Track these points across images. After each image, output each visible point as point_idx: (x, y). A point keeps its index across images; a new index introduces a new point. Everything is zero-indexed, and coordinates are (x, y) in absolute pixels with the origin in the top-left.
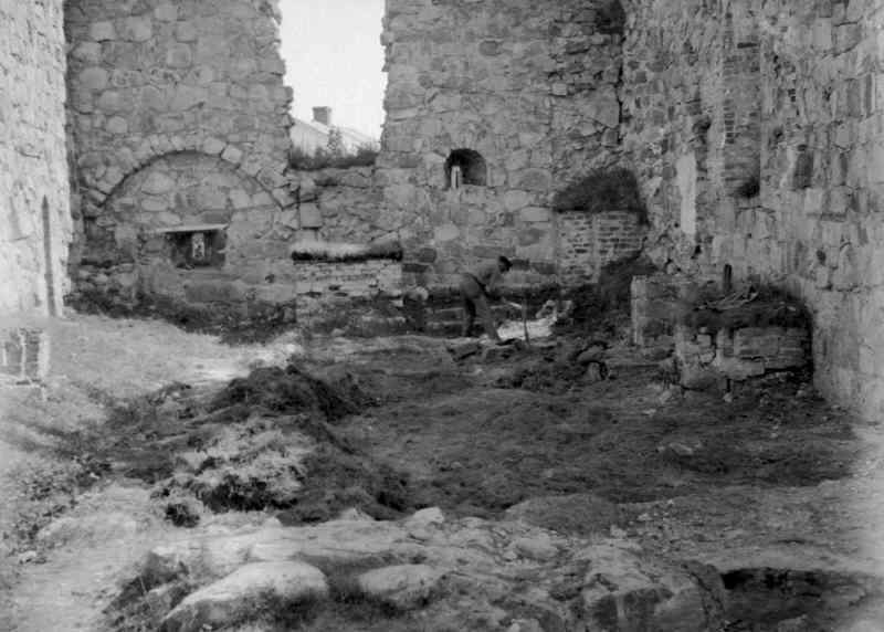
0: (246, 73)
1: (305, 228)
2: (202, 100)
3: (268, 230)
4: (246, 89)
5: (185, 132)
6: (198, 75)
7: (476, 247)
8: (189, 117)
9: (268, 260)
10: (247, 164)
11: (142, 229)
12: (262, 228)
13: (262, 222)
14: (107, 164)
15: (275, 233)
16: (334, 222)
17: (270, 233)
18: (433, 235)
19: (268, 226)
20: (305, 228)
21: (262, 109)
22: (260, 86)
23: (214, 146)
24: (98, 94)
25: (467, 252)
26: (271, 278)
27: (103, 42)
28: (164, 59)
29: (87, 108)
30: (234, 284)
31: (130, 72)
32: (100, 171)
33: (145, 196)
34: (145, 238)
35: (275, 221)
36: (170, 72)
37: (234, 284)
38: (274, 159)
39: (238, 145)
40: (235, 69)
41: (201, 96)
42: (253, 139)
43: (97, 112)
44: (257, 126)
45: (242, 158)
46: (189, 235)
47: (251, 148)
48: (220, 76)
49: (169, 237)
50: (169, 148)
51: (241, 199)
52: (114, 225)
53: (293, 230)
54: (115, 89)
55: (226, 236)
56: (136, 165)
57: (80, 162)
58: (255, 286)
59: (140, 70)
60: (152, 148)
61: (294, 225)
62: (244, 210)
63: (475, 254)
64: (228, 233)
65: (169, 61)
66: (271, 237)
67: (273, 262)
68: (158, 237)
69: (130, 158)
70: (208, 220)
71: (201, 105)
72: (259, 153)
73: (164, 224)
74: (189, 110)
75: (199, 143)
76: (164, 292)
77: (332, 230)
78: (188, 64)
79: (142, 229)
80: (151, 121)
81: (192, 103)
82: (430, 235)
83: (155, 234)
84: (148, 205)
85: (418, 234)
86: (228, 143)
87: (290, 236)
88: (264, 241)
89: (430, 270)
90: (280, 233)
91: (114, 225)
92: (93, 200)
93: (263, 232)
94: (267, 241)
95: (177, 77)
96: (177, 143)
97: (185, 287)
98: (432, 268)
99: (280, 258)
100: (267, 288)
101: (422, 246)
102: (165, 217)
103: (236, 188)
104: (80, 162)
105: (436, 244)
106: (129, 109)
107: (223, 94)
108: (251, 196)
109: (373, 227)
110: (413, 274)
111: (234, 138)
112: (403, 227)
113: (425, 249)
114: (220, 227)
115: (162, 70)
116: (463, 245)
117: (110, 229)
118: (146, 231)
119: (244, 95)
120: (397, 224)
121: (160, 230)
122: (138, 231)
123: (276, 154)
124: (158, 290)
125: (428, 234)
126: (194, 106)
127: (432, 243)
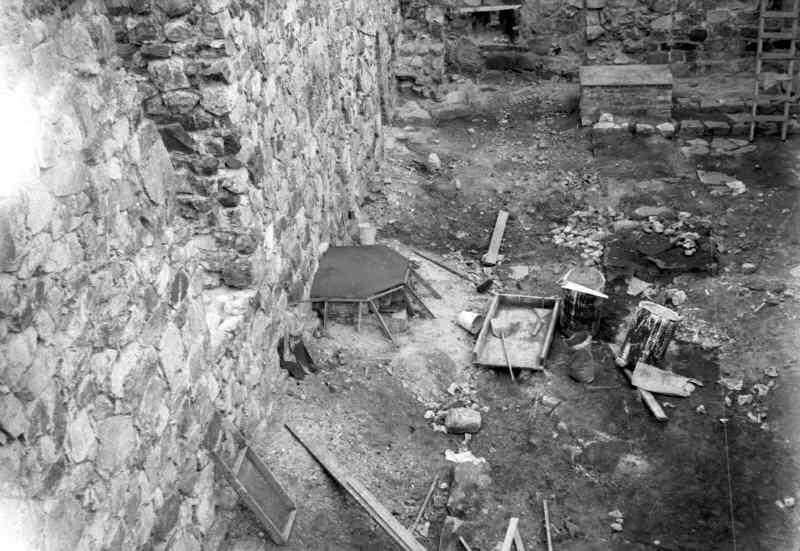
1: (590, 9)
3: (557, 9)
7: (743, 29)
9: (556, 35)
11: (448, 10)
12: (552, 8)
15: (563, 12)
17: (559, 12)
18: (705, 19)
20: (590, 9)
25: (735, 34)
26: (557, 51)
30: (526, 55)
34: (451, 17)
37: (526, 55)
46: (487, 14)
53: (578, 9)
58: (544, 57)
63: (742, 35)
64: (522, 12)
66: (559, 15)
67: (559, 36)
68: (463, 17)
76: (468, 61)
77: (614, 10)
79: (448, 10)
82: (702, 18)
83: (459, 14)
85: (691, 16)
88: (552, 20)
89: (700, 49)
90: (567, 12)
91: (425, 7)
93: (553, 12)
94: (556, 19)
97: (485, 57)
98: (701, 46)
100: (555, 59)
101: (695, 27)
105: (708, 26)
109: (652, 10)
110: (683, 52)
112: (678, 11)
113: (696, 30)
116: (732, 26)
117: (422, 10)
118: (451, 11)
120: (672, 9)
122: (445, 11)
124: (460, 59)
125: (702, 17)
127: (704, 25)
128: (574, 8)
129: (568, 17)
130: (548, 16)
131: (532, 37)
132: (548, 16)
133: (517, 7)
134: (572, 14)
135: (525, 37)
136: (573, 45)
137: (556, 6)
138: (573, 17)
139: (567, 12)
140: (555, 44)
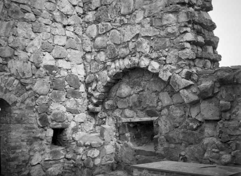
0: (161, 8)
1: (207, 121)
2: (137, 32)
3: (184, 120)
4: (161, 19)
5: (130, 56)
6: (135, 15)
8: (131, 45)
9: (183, 144)
10: (162, 73)
13: (179, 115)
14: (97, 81)
16: (228, 115)
17: (184, 124)
19: (182, 119)
21: (169, 30)
22: (171, 15)
23: (144, 63)
24: (93, 40)
27: (96, 9)
28: (120, 12)
29: (88, 49)
31: (105, 23)
32: (94, 85)
33: (119, 99)
35: (187, 115)
36: (123, 18)
38: (179, 67)
39: (157, 59)
40: (156, 8)
41: (137, 29)
42: (166, 54)
43: (93, 50)
44: (168, 44)
45: (160, 68)
47: (165, 61)
48: (146, 14)
49: (131, 125)
50: (123, 67)
51: (165, 99)
52: (105, 117)
54: (99, 35)
55: (158, 126)
56: (109, 79)
57: (86, 80)
59: (110, 22)
60: (115, 68)
61: (200, 119)
62: (168, 107)
64: (159, 124)
65: (122, 12)
66: (185, 127)
67: (186, 146)
69: (106, 76)
70: (151, 113)
71: (137, 36)
72: (170, 64)
73: (126, 117)
74: (131, 39)
75: (137, 61)
78: (131, 11)
79: (117, 121)
80: (114, 51)
81: (133, 36)
84: (120, 105)
86: (152, 59)
87: (198, 127)
90: (191, 124)
92: (92, 102)
95: (126, 21)
96: (126, 63)
99: (192, 144)
102: (128, 112)
103: (162, 91)
104: (86, 80)
106: (105, 45)
107: (149, 25)
108: (171, 96)
111: (154, 55)
114: (154, 118)
115: (119, 18)
119: (158, 24)
121: (124, 120)
123: (180, 63)
126: (133, 38)
128: (195, 120)
129: (193, 129)
130: (178, 127)
131: (166, 145)
132: (178, 127)
133: (154, 118)
134: (195, 127)
135: (162, 145)
136: (196, 155)
137: (182, 119)
138: (196, 129)
139: (191, 124)
140: (183, 153)
